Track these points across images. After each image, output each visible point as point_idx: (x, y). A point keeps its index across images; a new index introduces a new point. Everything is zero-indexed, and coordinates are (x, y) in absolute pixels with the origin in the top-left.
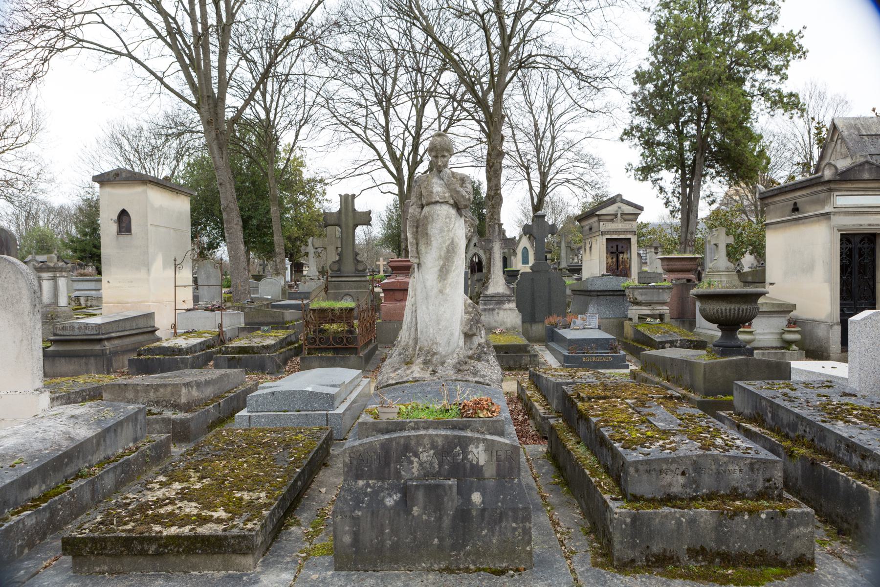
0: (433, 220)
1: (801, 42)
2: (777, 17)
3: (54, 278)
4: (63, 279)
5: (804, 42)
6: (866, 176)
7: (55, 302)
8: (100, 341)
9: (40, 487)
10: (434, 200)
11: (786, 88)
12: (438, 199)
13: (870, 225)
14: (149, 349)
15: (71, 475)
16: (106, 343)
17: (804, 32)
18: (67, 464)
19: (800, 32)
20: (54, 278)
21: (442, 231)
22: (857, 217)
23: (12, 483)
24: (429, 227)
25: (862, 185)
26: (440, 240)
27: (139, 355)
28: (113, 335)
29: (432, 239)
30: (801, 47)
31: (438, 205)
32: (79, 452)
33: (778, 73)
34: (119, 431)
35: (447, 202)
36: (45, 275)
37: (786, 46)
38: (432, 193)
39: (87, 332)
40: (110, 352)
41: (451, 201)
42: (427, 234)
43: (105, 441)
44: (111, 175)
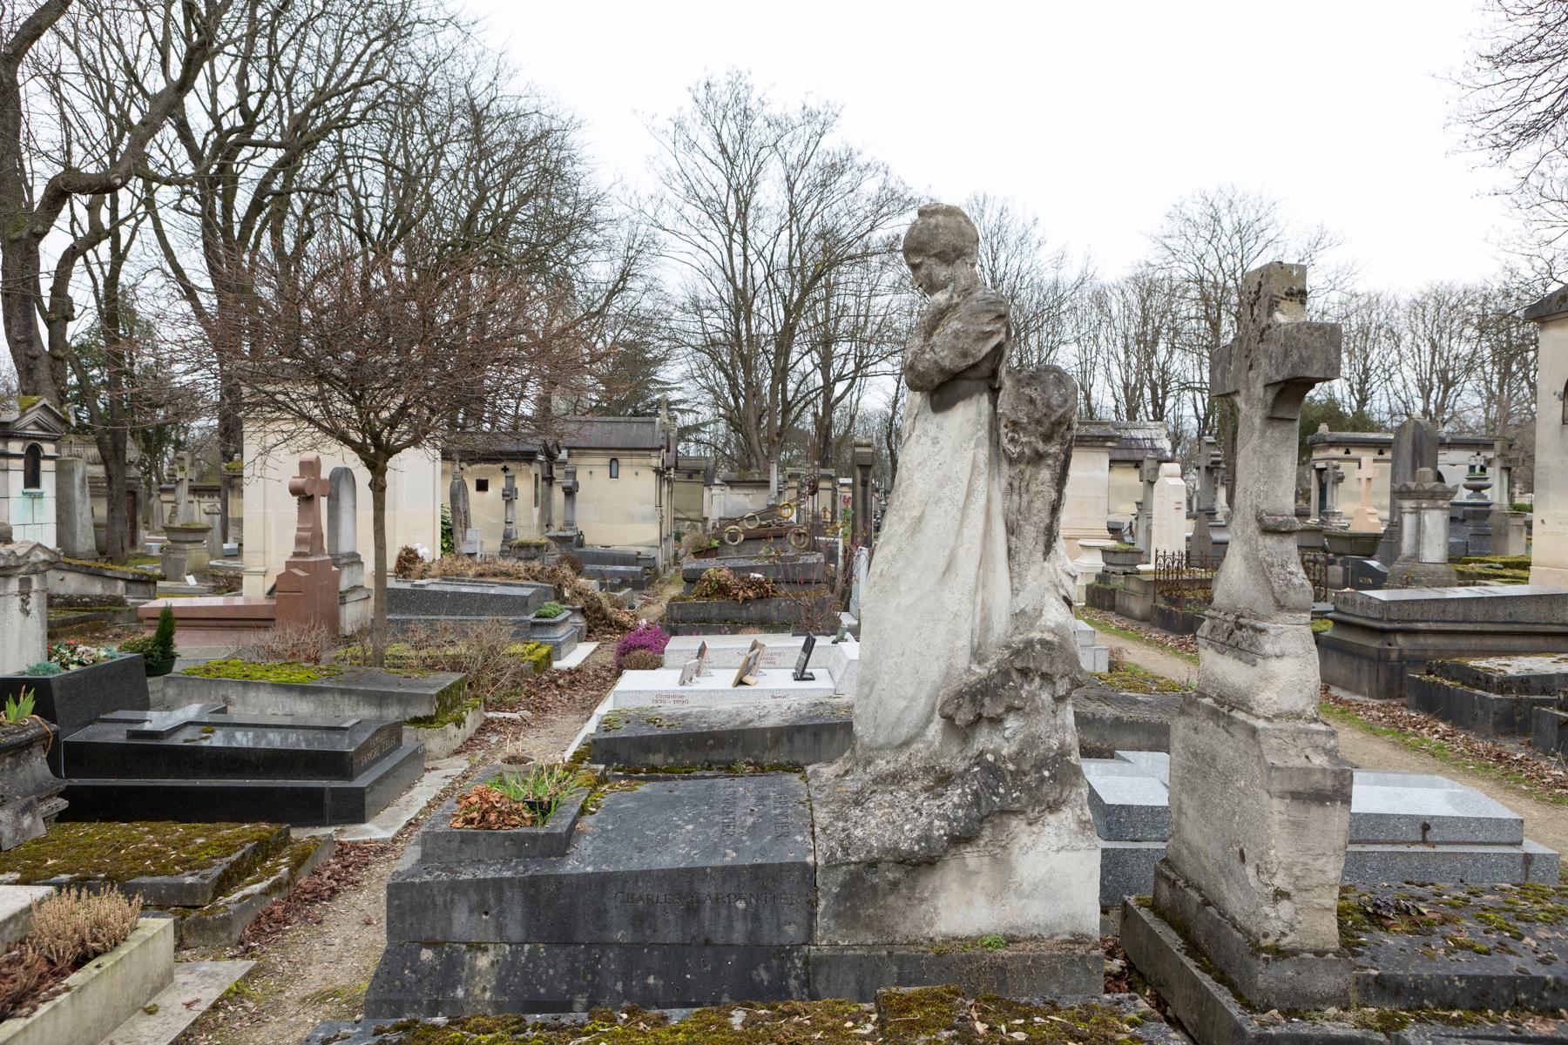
3: (1417, 511)
4: (1436, 513)
7: (1416, 556)
8: (1383, 632)
9: (666, 758)
14: (1443, 665)
15: (719, 762)
16: (1400, 640)
18: (712, 748)
20: (1417, 511)
23: (625, 739)
27: (1429, 673)
28: (1421, 626)
32: (736, 740)
34: (825, 736)
36: (1408, 504)
39: (1371, 614)
40: (1401, 658)
43: (790, 740)
44: (1555, 299)
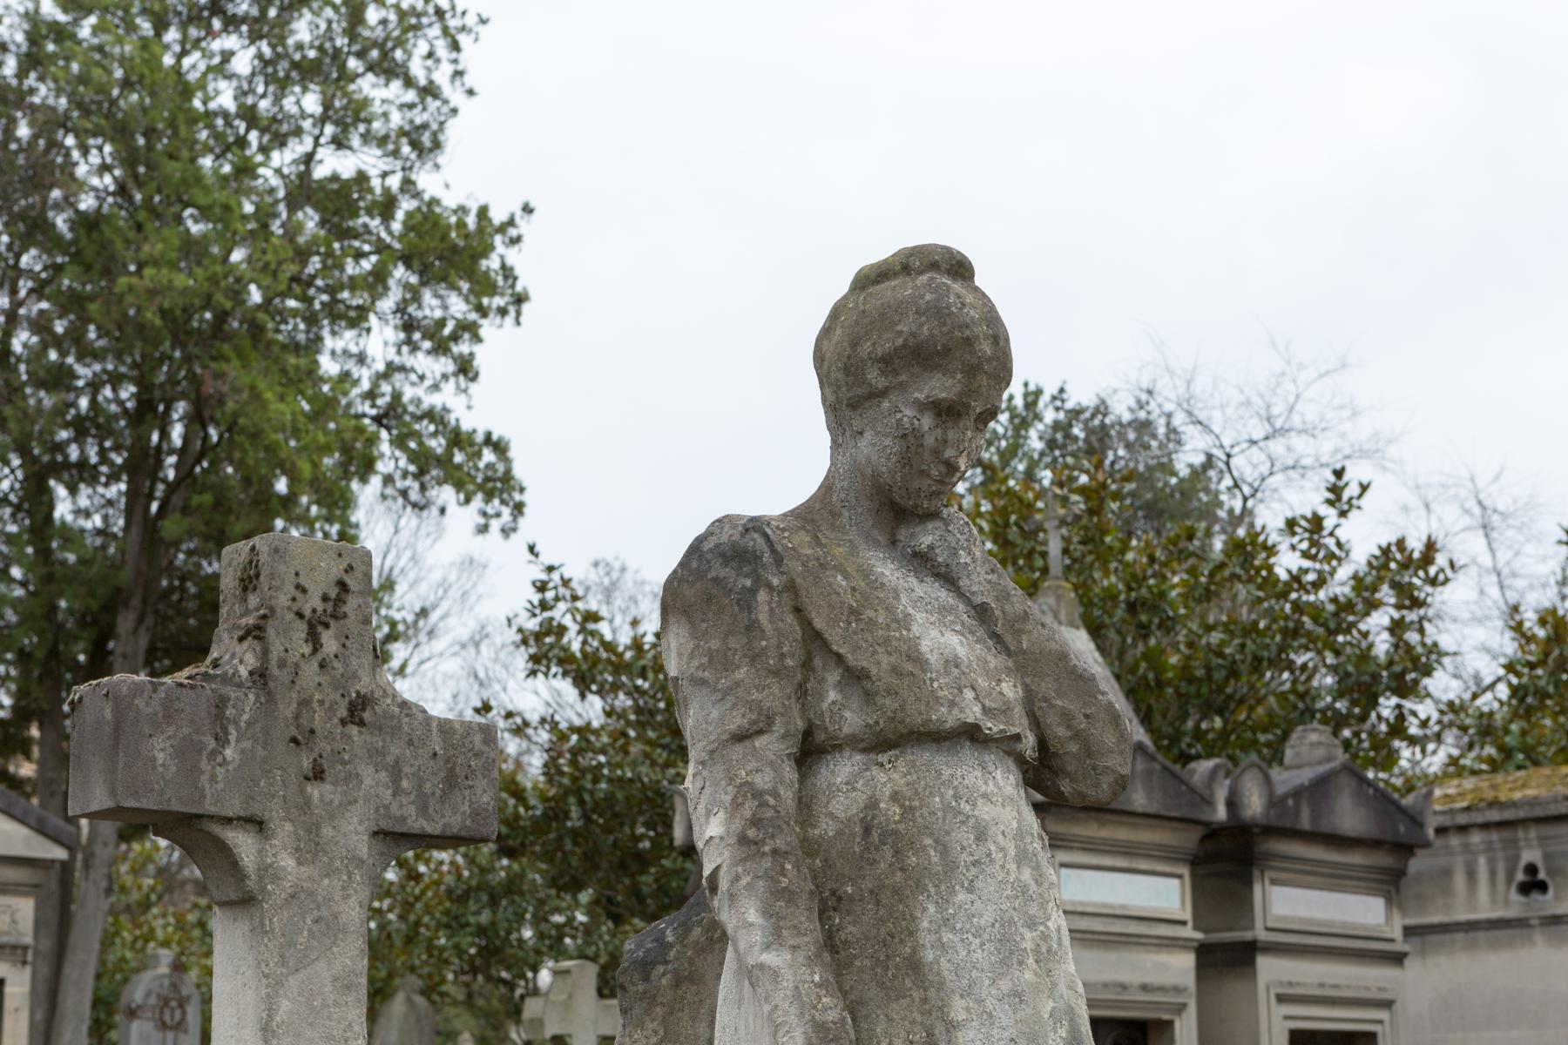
0: (950, 867)
1: (513, 257)
2: (437, 145)
5: (527, 260)
6: (1139, 799)
10: (949, 718)
11: (474, 411)
12: (973, 713)
13: (1145, 988)
17: (523, 226)
19: (511, 222)
21: (1008, 954)
22: (1112, 956)
24: (928, 916)
25: (1121, 833)
26: (1004, 1014)
29: (958, 1009)
30: (507, 272)
31: (967, 752)
33: (440, 348)
35: (1007, 744)
37: (456, 254)
38: (918, 659)
41: (1029, 743)
42: (914, 965)
